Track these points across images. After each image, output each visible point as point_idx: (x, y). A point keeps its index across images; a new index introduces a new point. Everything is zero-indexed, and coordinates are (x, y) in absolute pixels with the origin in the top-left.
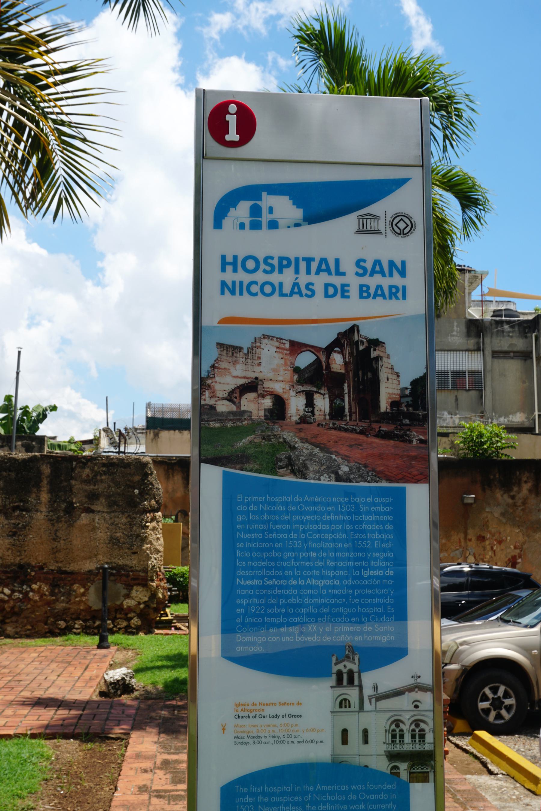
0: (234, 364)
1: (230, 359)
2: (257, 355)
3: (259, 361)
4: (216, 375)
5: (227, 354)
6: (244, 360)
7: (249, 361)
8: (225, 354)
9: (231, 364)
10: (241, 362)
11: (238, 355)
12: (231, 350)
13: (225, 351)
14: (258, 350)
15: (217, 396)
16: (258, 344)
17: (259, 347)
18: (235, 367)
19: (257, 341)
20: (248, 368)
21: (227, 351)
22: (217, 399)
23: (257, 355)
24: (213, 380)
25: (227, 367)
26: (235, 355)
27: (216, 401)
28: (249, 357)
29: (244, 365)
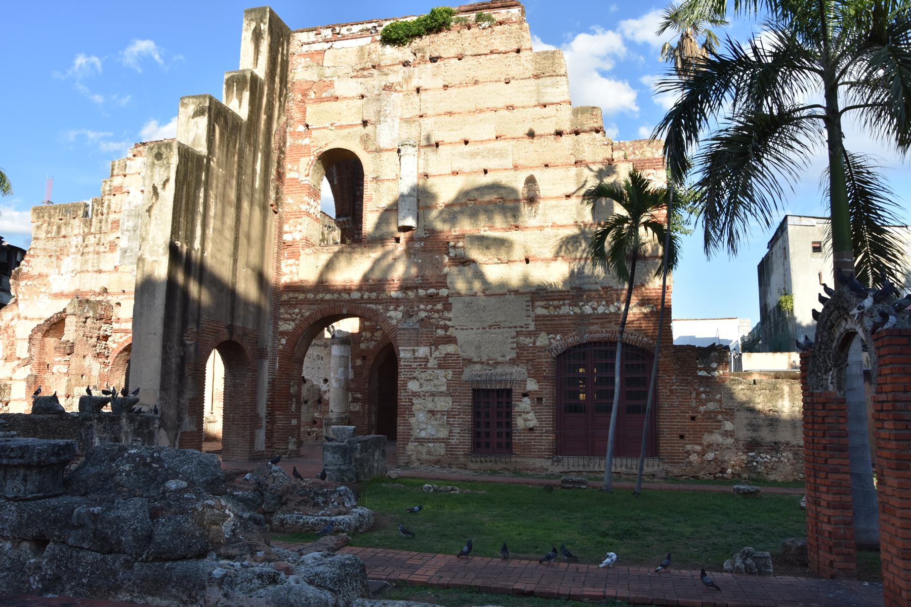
0: (58, 258)
1: (51, 245)
2: (112, 217)
3: (112, 237)
4: (20, 297)
5: (48, 232)
6: (80, 238)
7: (91, 240)
8: (42, 235)
9: (54, 259)
10: (73, 250)
11: (69, 229)
12: (56, 220)
13: (45, 225)
14: (115, 201)
15: (18, 355)
16: (117, 181)
17: (119, 189)
18: (58, 267)
19: (115, 172)
20: (86, 261)
21: (49, 224)
22: (17, 362)
23: (112, 217)
24: (15, 312)
25: (44, 270)
26: (63, 232)
27: (14, 371)
28: (93, 230)
29: (79, 257)
